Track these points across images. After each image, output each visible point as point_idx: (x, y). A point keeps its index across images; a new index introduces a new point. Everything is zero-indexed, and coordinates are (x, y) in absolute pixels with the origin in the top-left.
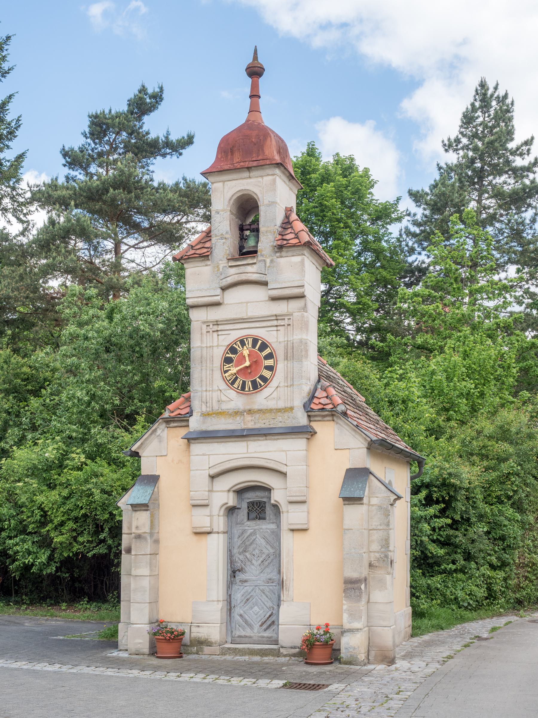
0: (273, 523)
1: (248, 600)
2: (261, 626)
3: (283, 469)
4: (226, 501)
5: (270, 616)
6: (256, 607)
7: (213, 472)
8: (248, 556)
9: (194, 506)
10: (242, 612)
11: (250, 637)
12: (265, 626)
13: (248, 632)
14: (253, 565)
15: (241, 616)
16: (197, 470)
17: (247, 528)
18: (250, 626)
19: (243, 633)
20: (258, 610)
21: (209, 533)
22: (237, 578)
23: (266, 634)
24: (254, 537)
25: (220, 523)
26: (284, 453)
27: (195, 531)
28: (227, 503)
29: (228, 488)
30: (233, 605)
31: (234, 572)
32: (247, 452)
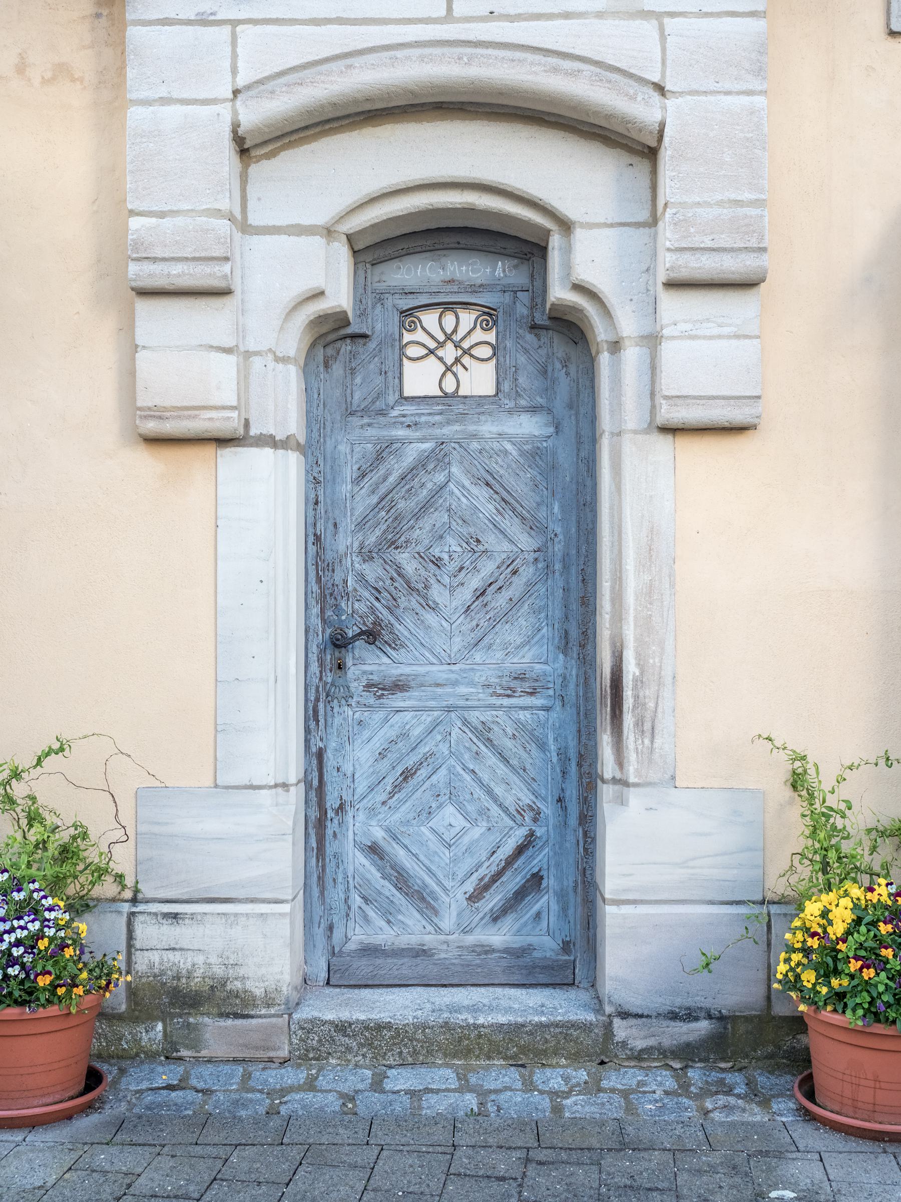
0: (533, 410)
1: (407, 775)
2: (474, 898)
3: (643, 110)
4: (318, 282)
5: (520, 850)
6: (450, 810)
7: (254, 114)
8: (410, 567)
9: (145, 293)
10: (378, 834)
11: (421, 953)
12: (494, 900)
13: (412, 929)
14: (435, 608)
15: (374, 850)
16: (165, 101)
17: (401, 433)
18: (423, 900)
19: (384, 934)
20: (459, 822)
21: (222, 441)
22: (353, 671)
23: (499, 937)
24: (440, 478)
25: (281, 400)
26: (649, 28)
27: (151, 427)
28: (320, 294)
29: (321, 218)
30: (332, 801)
31: (340, 639)
32: (449, 17)
